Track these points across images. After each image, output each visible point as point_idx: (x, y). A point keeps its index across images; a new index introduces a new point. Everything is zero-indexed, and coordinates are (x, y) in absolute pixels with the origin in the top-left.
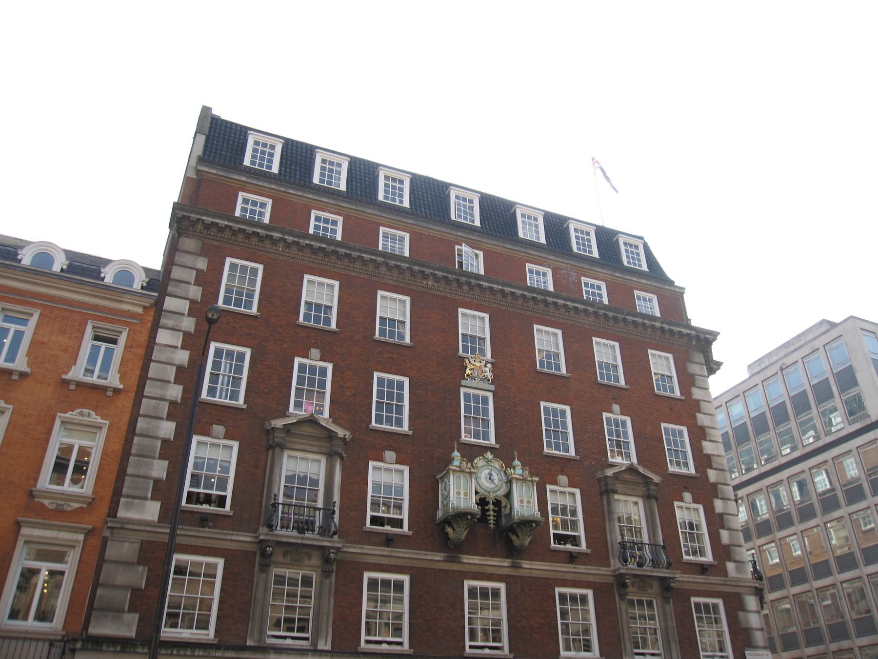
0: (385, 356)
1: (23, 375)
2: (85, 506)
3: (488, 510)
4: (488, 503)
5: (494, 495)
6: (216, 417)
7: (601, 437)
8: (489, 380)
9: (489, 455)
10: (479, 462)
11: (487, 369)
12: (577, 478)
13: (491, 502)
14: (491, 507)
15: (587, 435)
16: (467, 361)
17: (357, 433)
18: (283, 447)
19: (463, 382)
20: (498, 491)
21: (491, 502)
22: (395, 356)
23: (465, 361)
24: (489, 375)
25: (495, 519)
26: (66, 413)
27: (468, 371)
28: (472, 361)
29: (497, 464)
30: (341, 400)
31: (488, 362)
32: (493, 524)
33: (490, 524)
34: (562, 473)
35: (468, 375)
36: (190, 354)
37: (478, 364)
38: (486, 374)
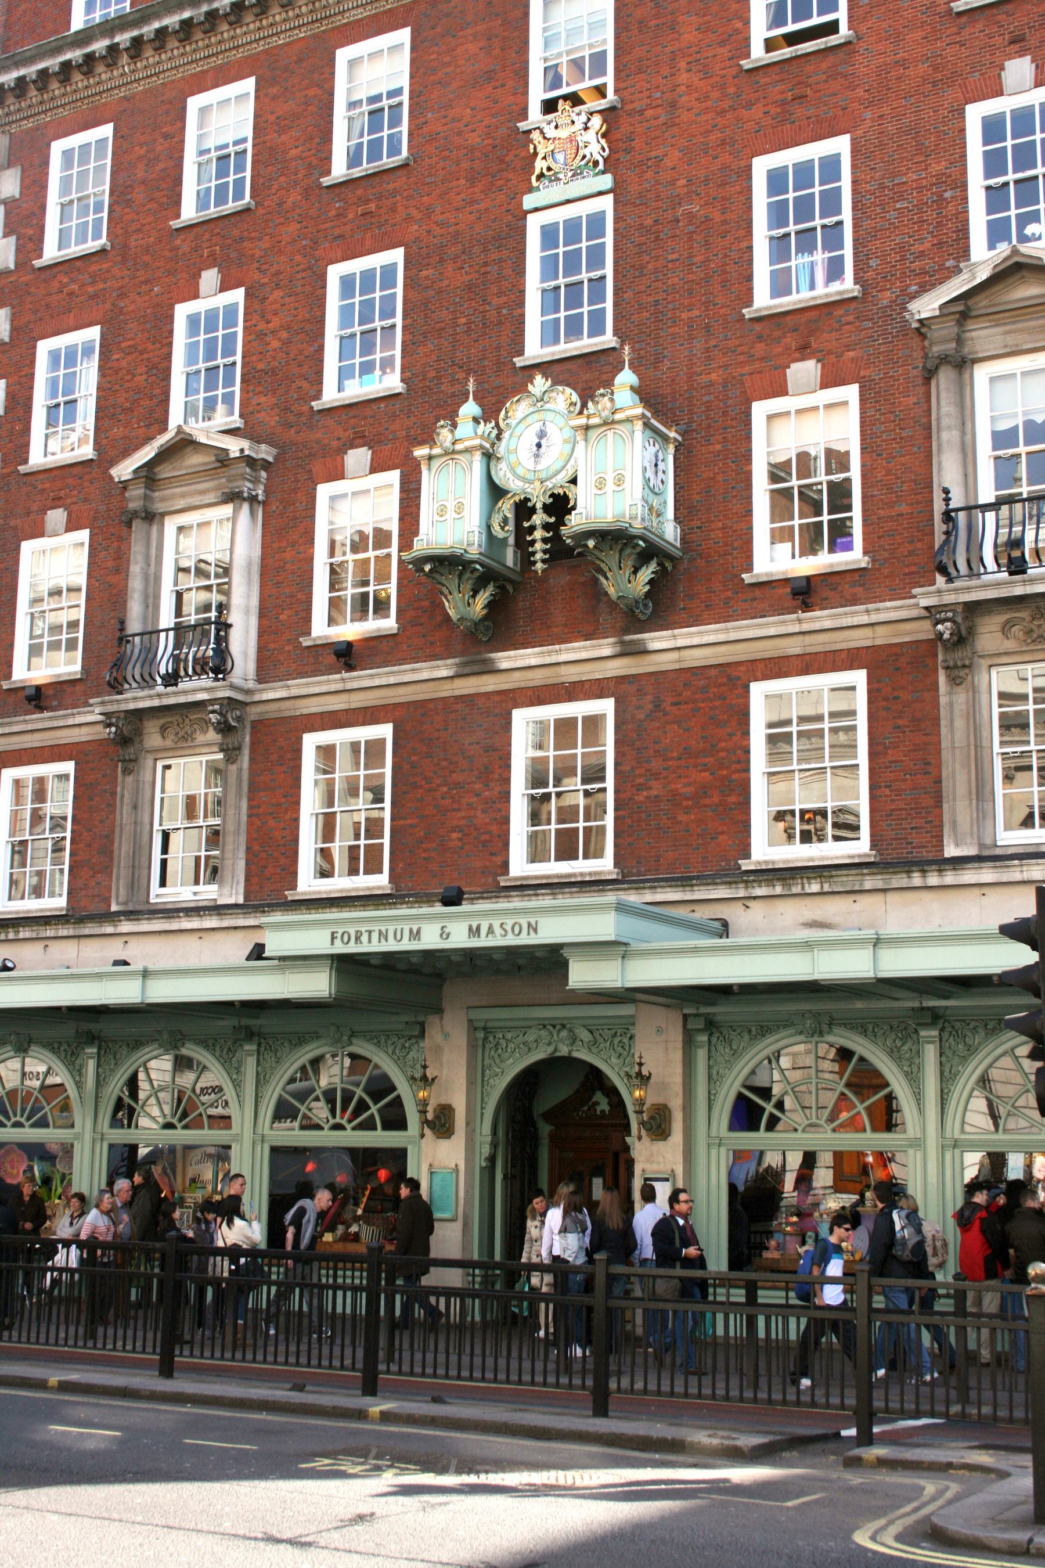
0: (351, 216)
3: (532, 529)
4: (533, 510)
7: (947, 195)
8: (596, 164)
9: (539, 384)
10: (518, 410)
11: (591, 136)
12: (851, 354)
13: (539, 506)
15: (898, 206)
16: (536, 136)
17: (293, 431)
18: (152, 517)
19: (529, 201)
20: (558, 472)
21: (539, 506)
22: (372, 206)
23: (532, 141)
24: (595, 147)
25: (548, 546)
27: (540, 165)
28: (550, 132)
29: (565, 397)
30: (261, 366)
31: (591, 114)
32: (544, 561)
33: (535, 563)
34: (803, 352)
35: (541, 176)
36: (8, 386)
37: (563, 133)
38: (587, 152)
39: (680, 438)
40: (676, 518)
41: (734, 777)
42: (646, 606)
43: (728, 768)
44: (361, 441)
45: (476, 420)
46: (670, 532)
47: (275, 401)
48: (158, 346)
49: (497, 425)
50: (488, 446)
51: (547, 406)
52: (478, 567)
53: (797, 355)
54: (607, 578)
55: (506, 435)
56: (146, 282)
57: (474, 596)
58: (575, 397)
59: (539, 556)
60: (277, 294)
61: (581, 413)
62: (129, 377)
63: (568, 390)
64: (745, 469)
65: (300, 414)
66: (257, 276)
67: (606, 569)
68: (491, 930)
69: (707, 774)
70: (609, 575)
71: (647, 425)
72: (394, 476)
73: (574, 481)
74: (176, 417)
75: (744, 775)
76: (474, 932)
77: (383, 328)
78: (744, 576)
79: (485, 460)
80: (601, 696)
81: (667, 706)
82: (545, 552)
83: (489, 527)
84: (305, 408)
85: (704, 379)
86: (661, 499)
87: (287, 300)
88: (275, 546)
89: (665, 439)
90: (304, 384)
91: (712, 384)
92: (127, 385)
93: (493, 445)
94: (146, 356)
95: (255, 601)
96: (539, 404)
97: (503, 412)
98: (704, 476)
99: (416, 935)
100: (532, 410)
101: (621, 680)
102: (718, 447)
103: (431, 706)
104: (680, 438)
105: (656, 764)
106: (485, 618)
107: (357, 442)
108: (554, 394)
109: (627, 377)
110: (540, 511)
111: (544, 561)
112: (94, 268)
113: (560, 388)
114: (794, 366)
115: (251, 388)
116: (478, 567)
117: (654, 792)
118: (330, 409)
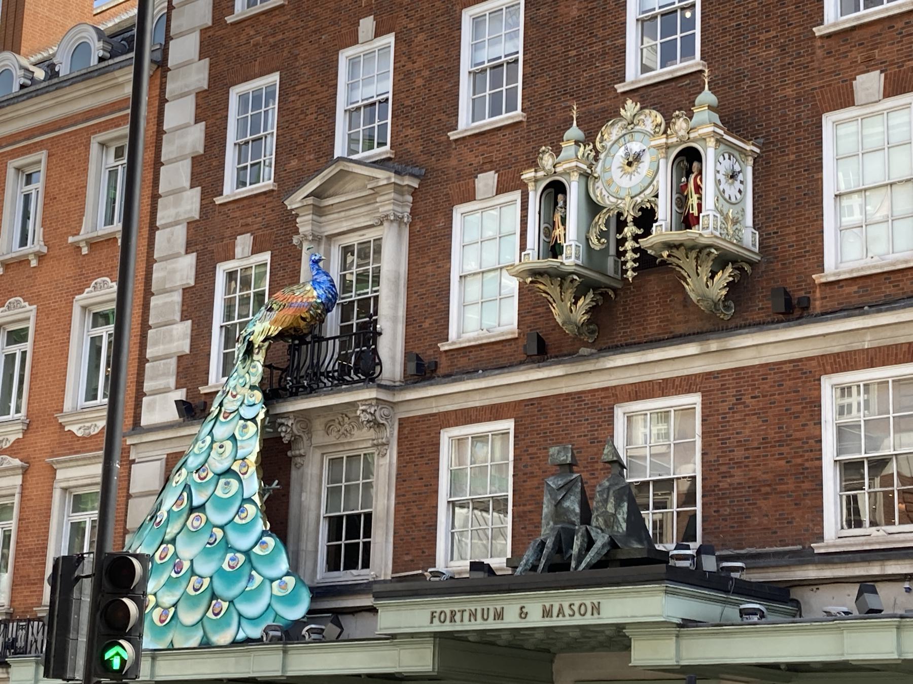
1: (40, 257)
2: (20, 436)
5: (639, 199)
6: (241, 221)
9: (630, 108)
10: (612, 133)
14: (630, 230)
21: (630, 219)
26: (83, 293)
29: (651, 119)
30: (408, 102)
32: (634, 269)
34: (868, 65)
39: (758, 151)
40: (755, 226)
41: (807, 465)
42: (727, 308)
43: (801, 456)
44: (488, 165)
45: (577, 143)
46: (749, 238)
47: (419, 132)
48: (325, 88)
49: (594, 147)
50: (585, 167)
51: (637, 128)
52: (575, 277)
53: (863, 67)
54: (688, 284)
55: (602, 156)
56: (315, 32)
57: (575, 303)
58: (660, 119)
59: (629, 265)
60: (421, 37)
61: (665, 132)
62: (302, 117)
63: (654, 112)
64: (816, 177)
65: (438, 144)
66: (405, 21)
67: (685, 275)
68: (561, 611)
69: (783, 462)
70: (689, 280)
71: (719, 141)
72: (517, 195)
73: (657, 196)
74: (340, 150)
75: (817, 462)
76: (547, 613)
77: (508, 63)
78: (814, 276)
79: (583, 180)
80: (689, 391)
81: (747, 400)
82: (635, 261)
83: (587, 239)
84: (443, 138)
85: (779, 95)
86: (738, 208)
87: (429, 42)
88: (419, 262)
89: (742, 151)
90: (443, 117)
91: (786, 98)
92: (301, 123)
93: (590, 166)
94: (316, 97)
95: (402, 312)
96: (630, 127)
97: (599, 135)
98: (780, 185)
99: (499, 616)
100: (624, 132)
101: (708, 375)
102: (792, 157)
103: (543, 402)
104: (758, 151)
105: (739, 454)
106: (589, 322)
107: (485, 167)
108: (642, 117)
109: (707, 97)
110: (631, 224)
111: (634, 269)
112: (275, 21)
113: (647, 111)
114: (860, 78)
115: (400, 122)
116: (575, 277)
117: (736, 480)
118: (464, 138)
